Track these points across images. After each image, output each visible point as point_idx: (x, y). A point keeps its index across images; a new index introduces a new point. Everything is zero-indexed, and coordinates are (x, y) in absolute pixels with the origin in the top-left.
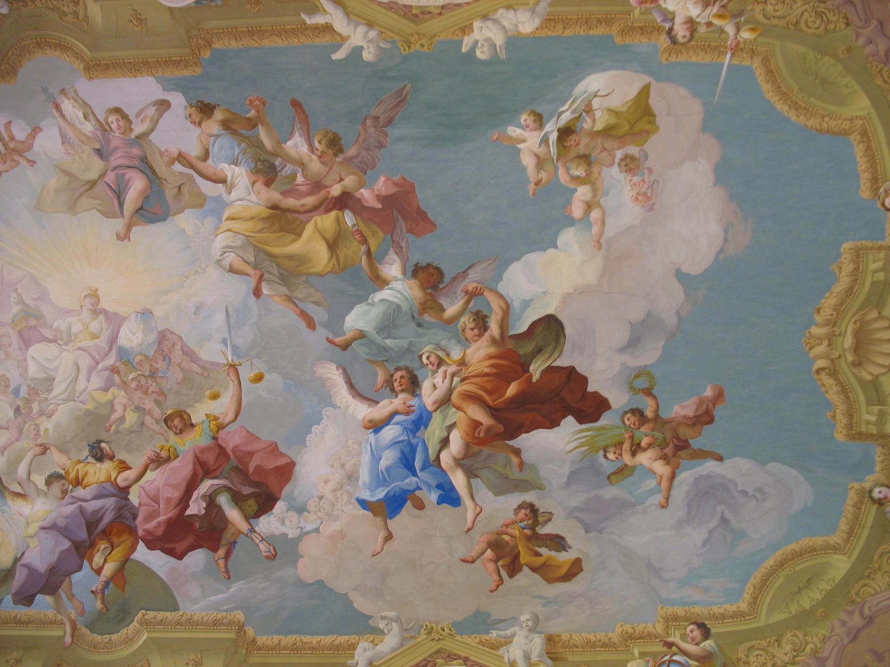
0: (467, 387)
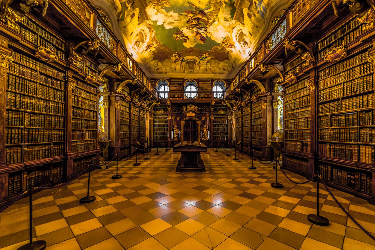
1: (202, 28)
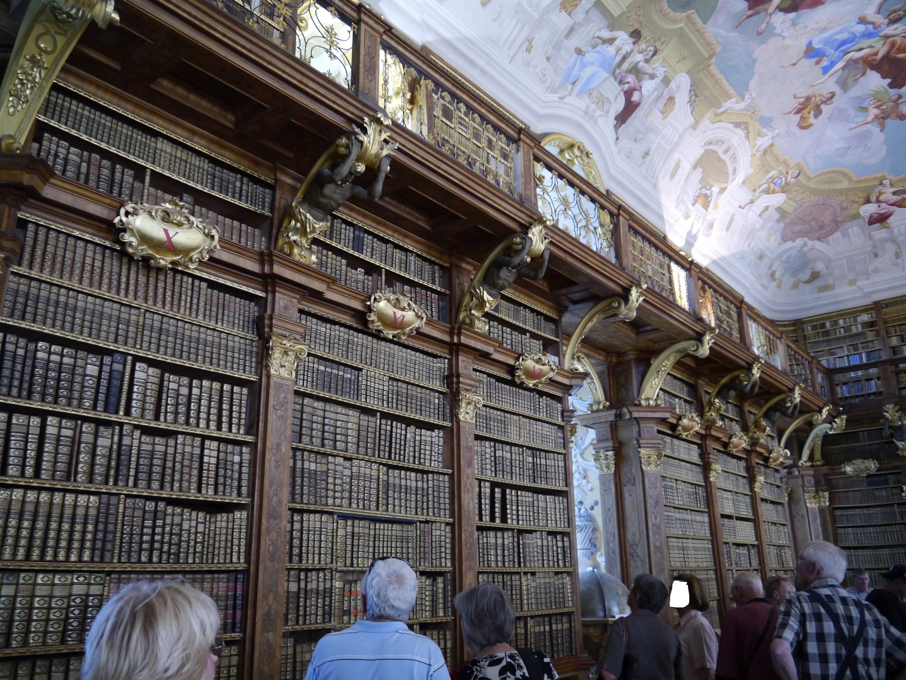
0: (899, 40)
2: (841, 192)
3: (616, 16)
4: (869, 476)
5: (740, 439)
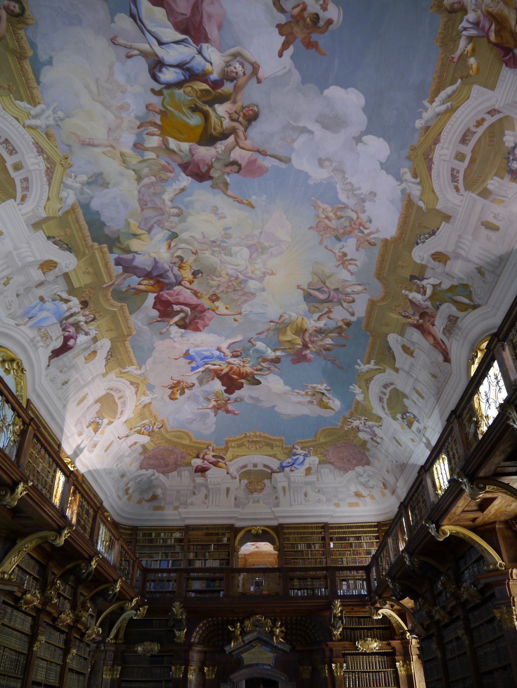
0: (235, 368)
1: (179, 85)
2: (184, 446)
3: (75, 287)
4: (152, 656)
5: (67, 616)
